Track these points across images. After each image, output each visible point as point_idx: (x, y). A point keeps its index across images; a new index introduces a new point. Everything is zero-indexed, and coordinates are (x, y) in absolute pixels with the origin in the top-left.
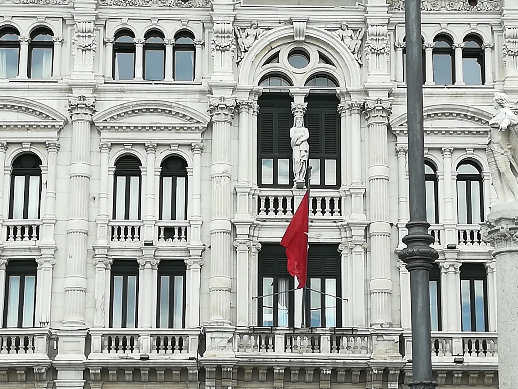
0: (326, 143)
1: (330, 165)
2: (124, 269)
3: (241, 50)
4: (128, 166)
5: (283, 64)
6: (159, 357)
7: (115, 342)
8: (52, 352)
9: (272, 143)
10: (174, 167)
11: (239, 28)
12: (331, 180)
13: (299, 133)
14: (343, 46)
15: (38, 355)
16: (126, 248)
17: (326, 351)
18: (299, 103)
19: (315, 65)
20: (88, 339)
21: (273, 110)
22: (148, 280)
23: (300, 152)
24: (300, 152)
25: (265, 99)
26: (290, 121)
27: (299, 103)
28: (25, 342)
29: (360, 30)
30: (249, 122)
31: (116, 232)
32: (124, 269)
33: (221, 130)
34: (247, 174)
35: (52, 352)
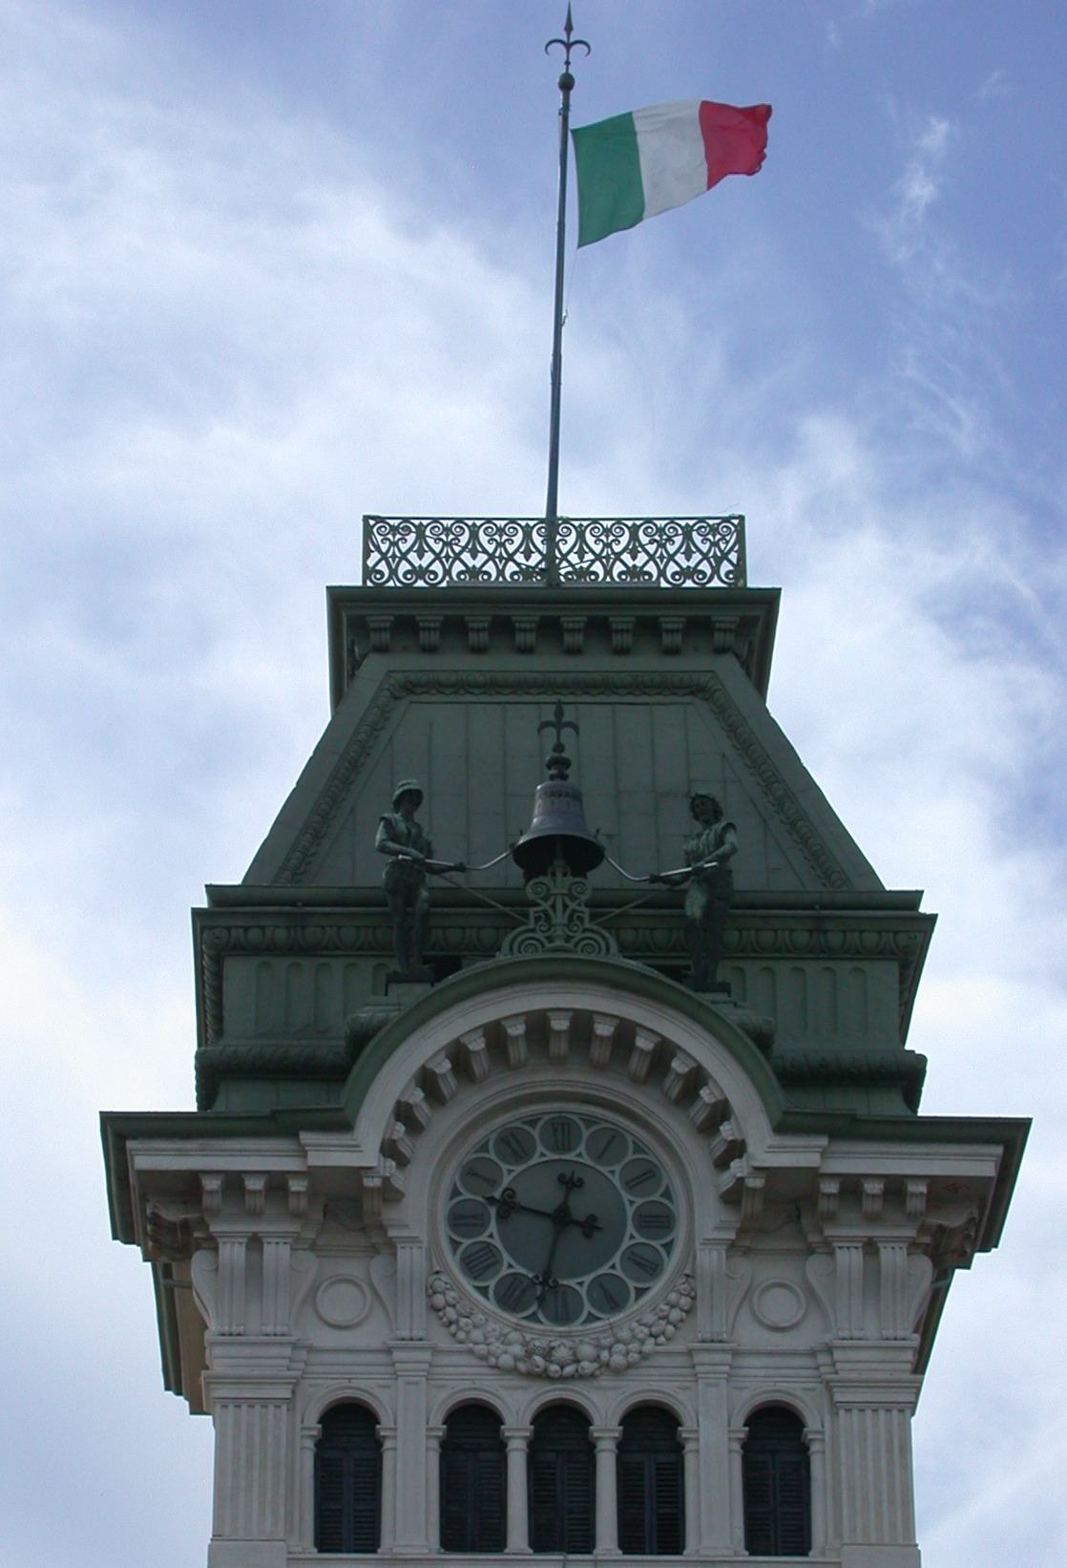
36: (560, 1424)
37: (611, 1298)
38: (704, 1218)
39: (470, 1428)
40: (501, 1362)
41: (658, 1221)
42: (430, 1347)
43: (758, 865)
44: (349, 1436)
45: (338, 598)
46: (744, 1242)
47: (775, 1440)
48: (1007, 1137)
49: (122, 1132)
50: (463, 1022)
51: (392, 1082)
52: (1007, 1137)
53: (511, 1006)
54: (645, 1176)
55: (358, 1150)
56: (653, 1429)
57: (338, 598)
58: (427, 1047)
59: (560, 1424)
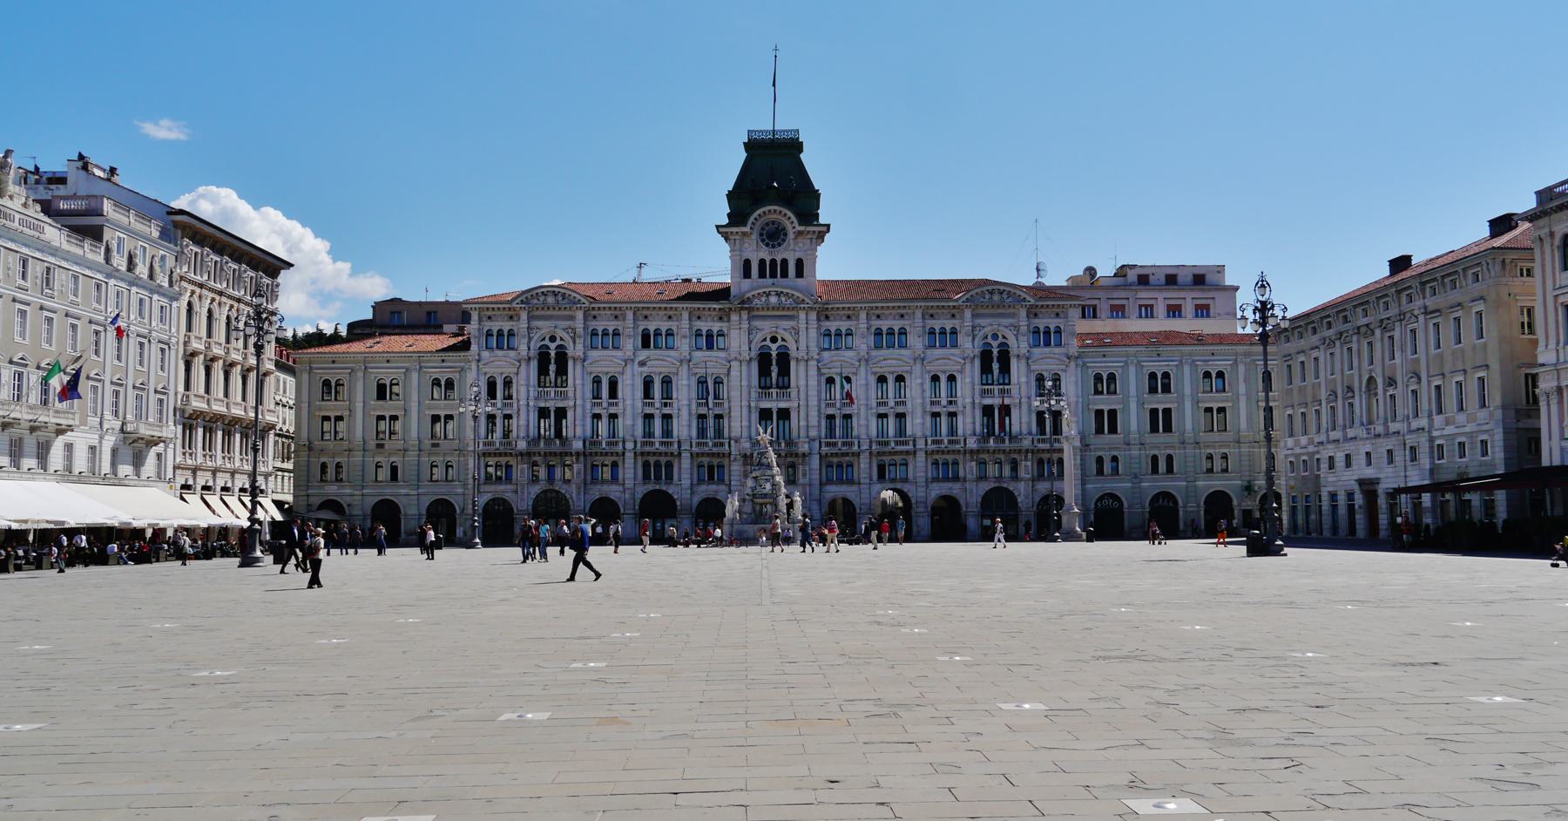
0: (1005, 369)
4: (935, 379)
5: (989, 340)
6: (952, 447)
7: (934, 442)
9: (986, 369)
10: (952, 378)
11: (974, 327)
13: (996, 366)
15: (911, 447)
16: (936, 409)
19: (1000, 339)
21: (986, 357)
22: (944, 419)
27: (995, 352)
28: (906, 443)
29: (1017, 328)
30: (977, 363)
31: (932, 403)
32: (936, 415)
33: (968, 366)
34: (977, 379)
36: (773, 261)
38: (791, 235)
39: (762, 262)
42: (758, 253)
47: (800, 264)
48: (828, 226)
50: (759, 211)
51: (752, 219)
52: (828, 226)
53: (766, 209)
55: (747, 229)
56: (785, 262)
58: (755, 215)
59: (773, 261)
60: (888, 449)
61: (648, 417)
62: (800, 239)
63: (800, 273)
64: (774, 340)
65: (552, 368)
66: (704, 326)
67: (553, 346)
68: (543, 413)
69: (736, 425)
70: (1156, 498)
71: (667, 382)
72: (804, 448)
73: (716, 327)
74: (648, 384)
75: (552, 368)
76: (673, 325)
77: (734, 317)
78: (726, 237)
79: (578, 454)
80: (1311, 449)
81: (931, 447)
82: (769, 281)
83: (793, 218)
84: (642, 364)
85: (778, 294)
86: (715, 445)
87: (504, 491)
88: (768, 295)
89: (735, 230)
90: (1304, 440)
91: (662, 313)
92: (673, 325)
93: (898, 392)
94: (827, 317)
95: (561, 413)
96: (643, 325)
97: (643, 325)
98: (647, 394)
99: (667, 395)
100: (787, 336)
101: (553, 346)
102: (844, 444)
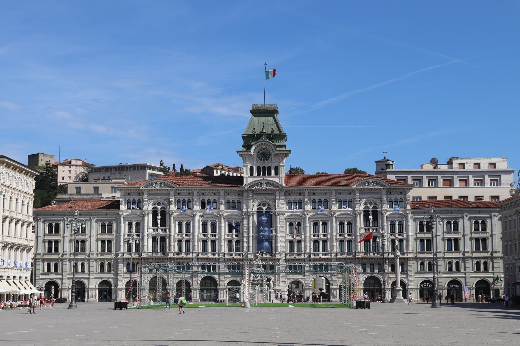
0: (375, 219)
1: (376, 222)
2: (342, 241)
3: (360, 203)
7: (341, 254)
8: (331, 256)
9: (366, 219)
12: (376, 225)
13: (371, 217)
14: (378, 202)
15: (329, 257)
17: (376, 256)
18: (371, 212)
20: (337, 253)
23: (371, 221)
24: (371, 221)
25: (364, 211)
26: (369, 215)
34: (362, 226)
35: (331, 256)
36: (264, 167)
37: (267, 160)
38: (272, 155)
40: (261, 164)
41: (270, 155)
43: (276, 132)
44: (251, 169)
45: (250, 111)
46: (275, 156)
49: (238, 152)
51: (253, 148)
52: (290, 151)
53: (260, 143)
54: (269, 152)
57: (250, 111)
59: (264, 167)
60: (318, 257)
61: (205, 242)
62: (277, 157)
63: (277, 173)
64: (264, 205)
65: (159, 217)
66: (231, 198)
67: (159, 208)
68: (154, 239)
69: (245, 244)
70: (450, 283)
71: (213, 225)
72: (278, 257)
73: (237, 198)
74: (205, 225)
75: (159, 217)
76: (216, 197)
77: (245, 194)
78: (241, 156)
79: (171, 259)
80: (514, 262)
81: (339, 256)
82: (261, 178)
83: (273, 148)
84: (202, 216)
85: (266, 184)
86: (236, 255)
87: (135, 276)
88: (262, 184)
89: (246, 153)
90: (511, 257)
91: (211, 192)
92: (216, 197)
93: (325, 231)
94: (289, 194)
95: (163, 239)
96: (202, 198)
97: (202, 198)
98: (205, 230)
99: (213, 231)
100: (270, 202)
101: (159, 208)
102: (298, 255)
